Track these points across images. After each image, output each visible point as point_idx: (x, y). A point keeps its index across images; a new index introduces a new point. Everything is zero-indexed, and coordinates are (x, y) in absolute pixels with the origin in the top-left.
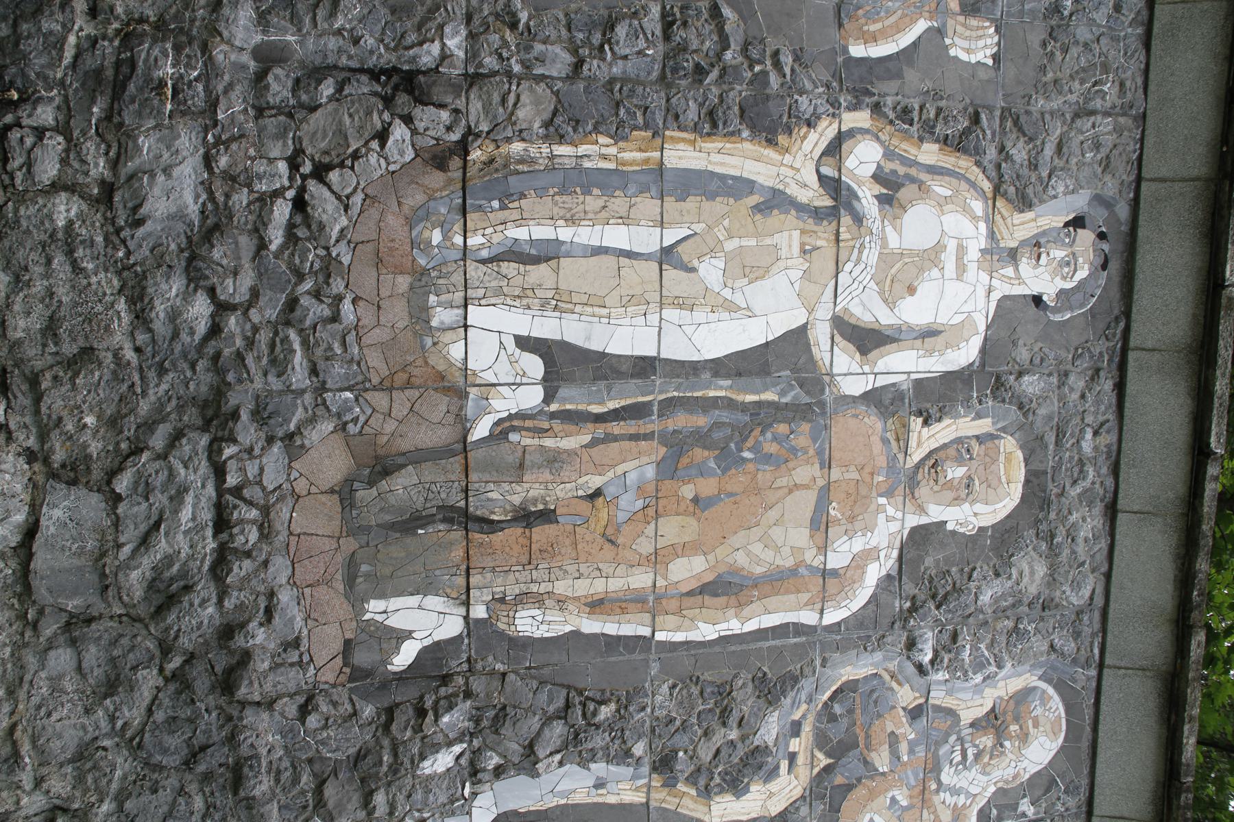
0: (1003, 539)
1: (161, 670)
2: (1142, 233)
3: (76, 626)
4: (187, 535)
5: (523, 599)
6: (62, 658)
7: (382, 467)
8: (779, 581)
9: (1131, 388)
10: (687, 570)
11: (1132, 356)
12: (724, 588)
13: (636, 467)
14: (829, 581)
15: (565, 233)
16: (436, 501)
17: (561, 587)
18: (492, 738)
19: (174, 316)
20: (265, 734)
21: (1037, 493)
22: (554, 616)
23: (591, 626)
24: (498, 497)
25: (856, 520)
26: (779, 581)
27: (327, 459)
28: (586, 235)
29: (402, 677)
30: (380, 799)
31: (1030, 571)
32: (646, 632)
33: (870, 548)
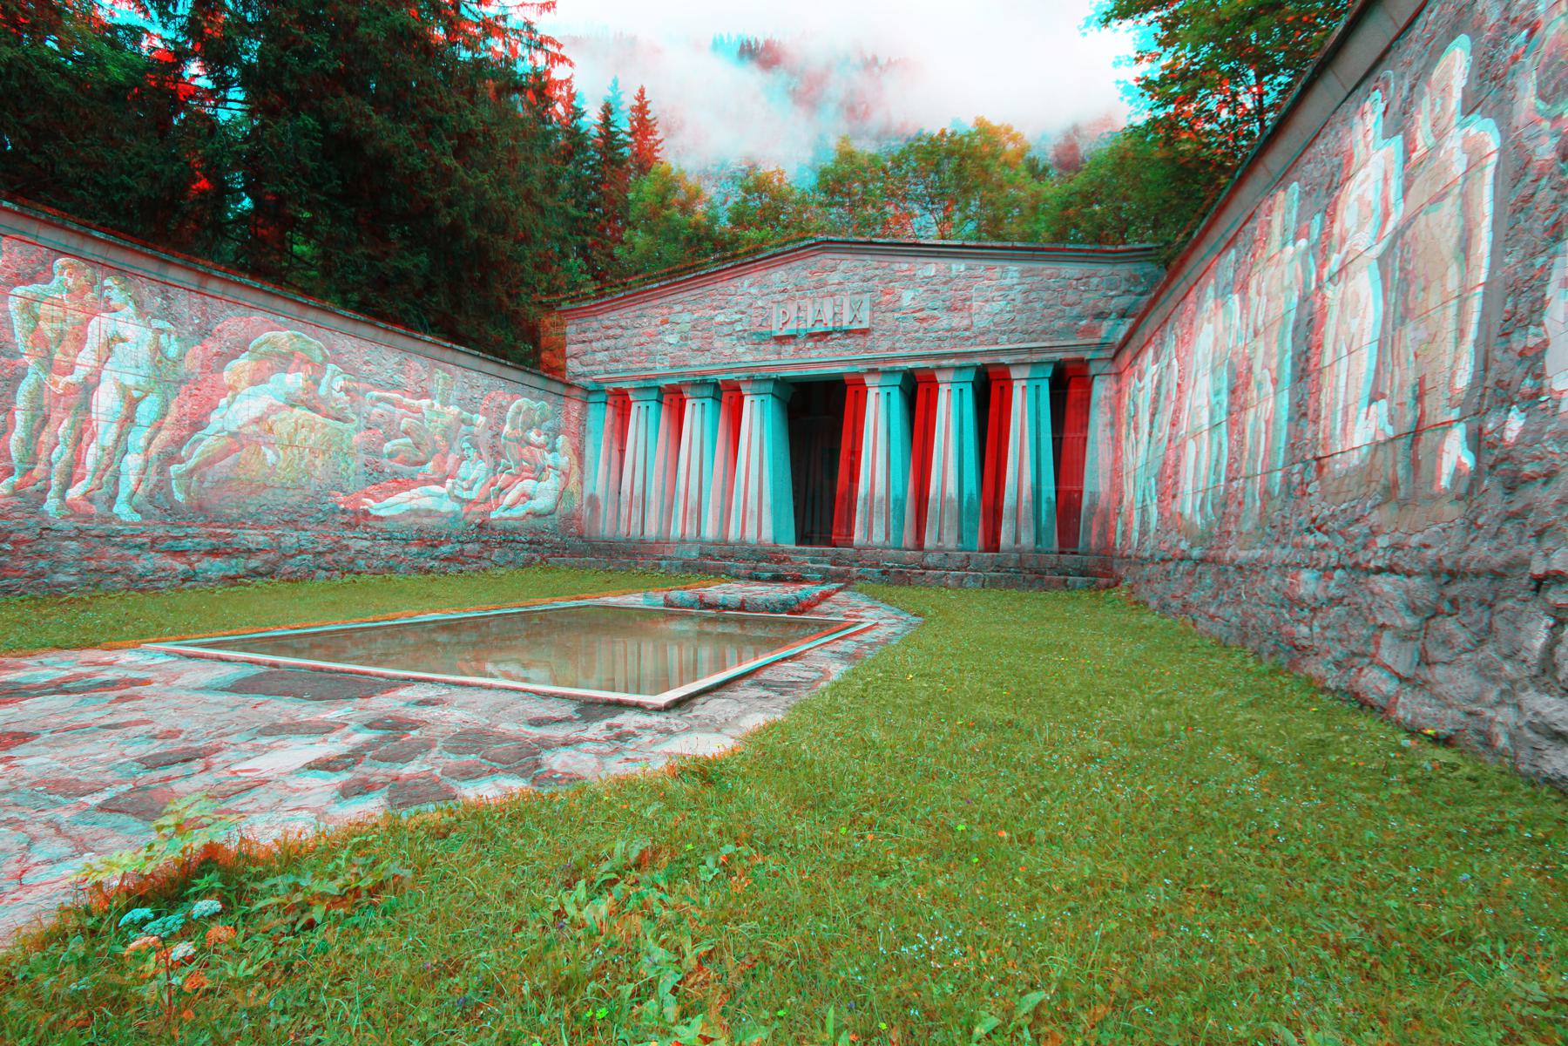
1: (1450, 615)
2: (1361, 74)
3: (1425, 661)
5: (1451, 385)
6: (1440, 672)
9: (1411, 11)
11: (1401, 26)
12: (1465, 246)
15: (1340, 406)
17: (1448, 363)
18: (1513, 388)
19: (1339, 586)
20: (1483, 551)
22: (1462, 364)
23: (1472, 332)
28: (1341, 397)
29: (1478, 460)
30: (1527, 469)
32: (1480, 290)
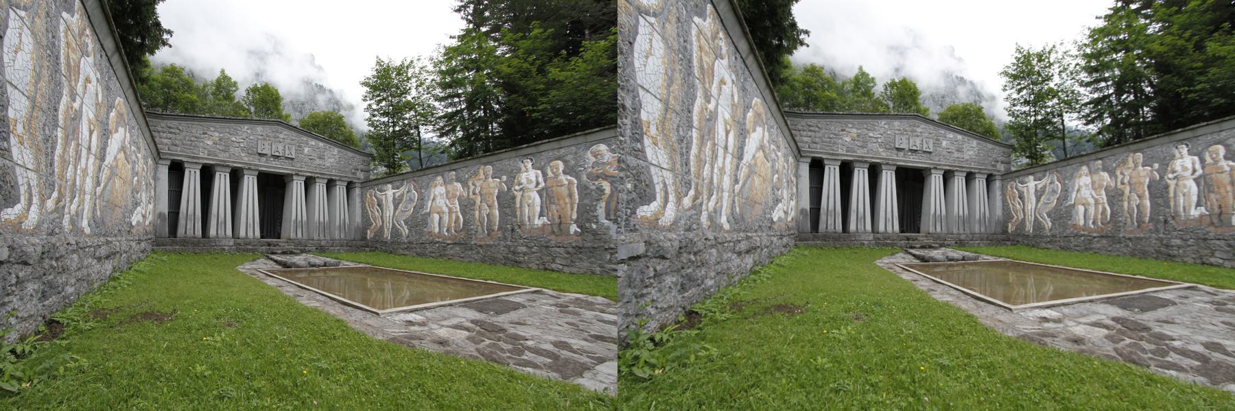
0: (565, 162)
4: (562, 250)
7: (553, 232)
8: (569, 189)
10: (567, 200)
12: (571, 195)
13: (553, 207)
14: (570, 183)
16: (560, 226)
21: (559, 159)
24: (557, 221)
25: (561, 181)
26: (569, 189)
27: (553, 237)
31: (569, 157)
33: (564, 179)
